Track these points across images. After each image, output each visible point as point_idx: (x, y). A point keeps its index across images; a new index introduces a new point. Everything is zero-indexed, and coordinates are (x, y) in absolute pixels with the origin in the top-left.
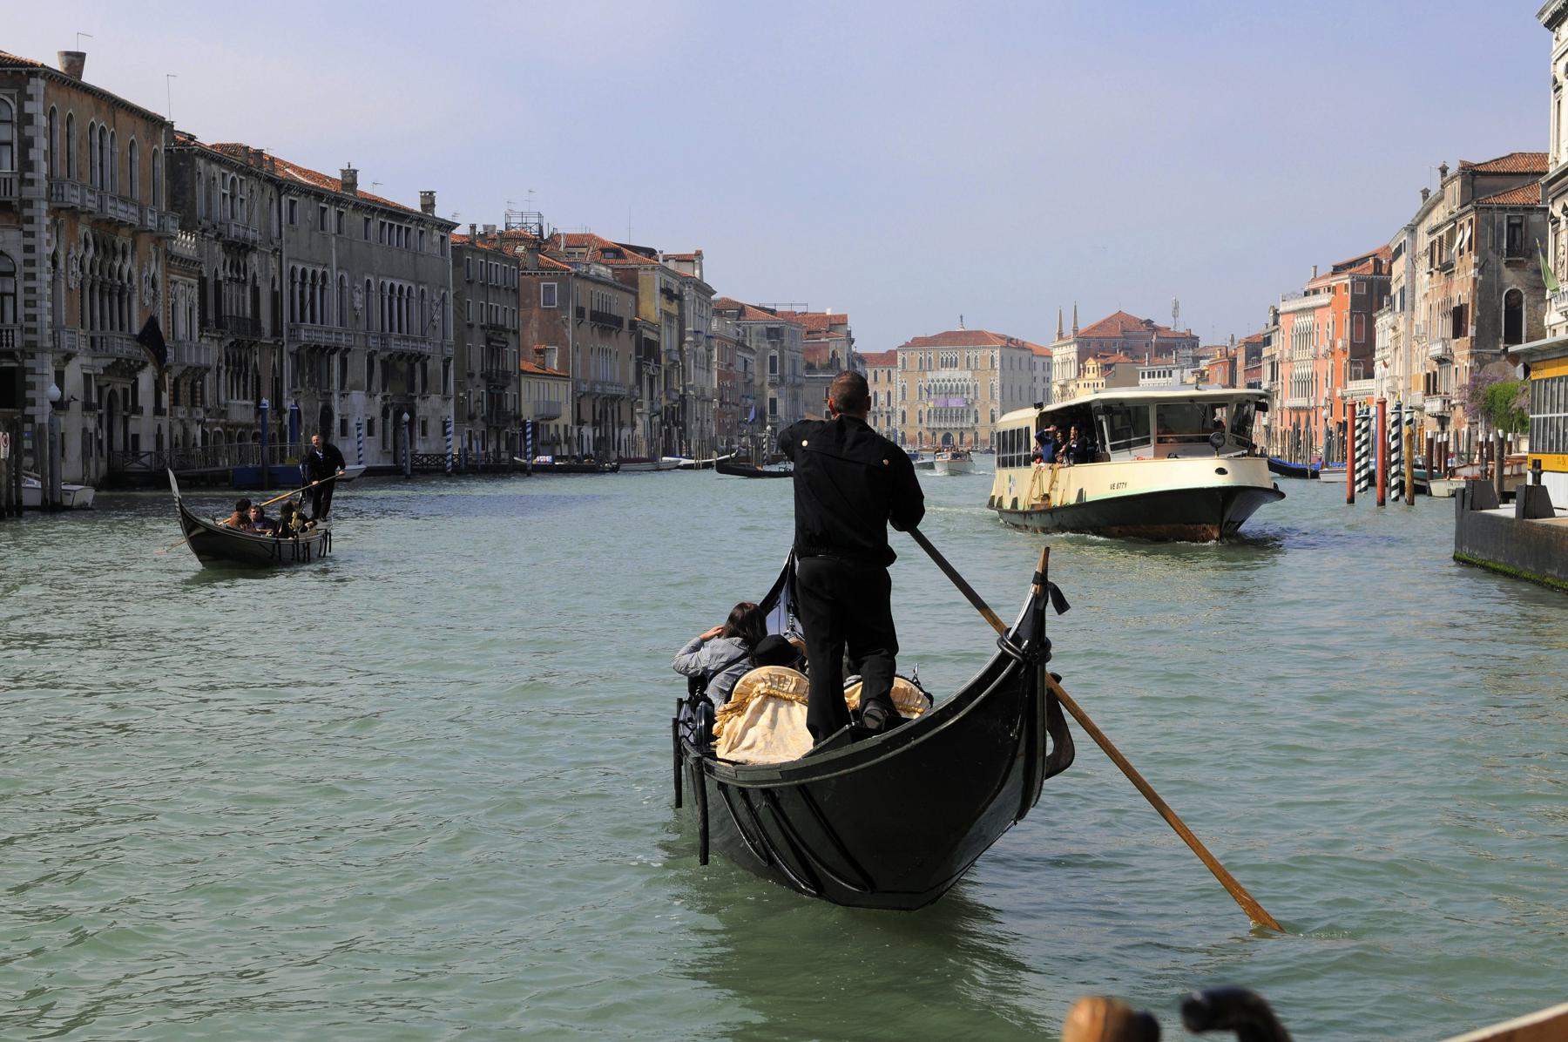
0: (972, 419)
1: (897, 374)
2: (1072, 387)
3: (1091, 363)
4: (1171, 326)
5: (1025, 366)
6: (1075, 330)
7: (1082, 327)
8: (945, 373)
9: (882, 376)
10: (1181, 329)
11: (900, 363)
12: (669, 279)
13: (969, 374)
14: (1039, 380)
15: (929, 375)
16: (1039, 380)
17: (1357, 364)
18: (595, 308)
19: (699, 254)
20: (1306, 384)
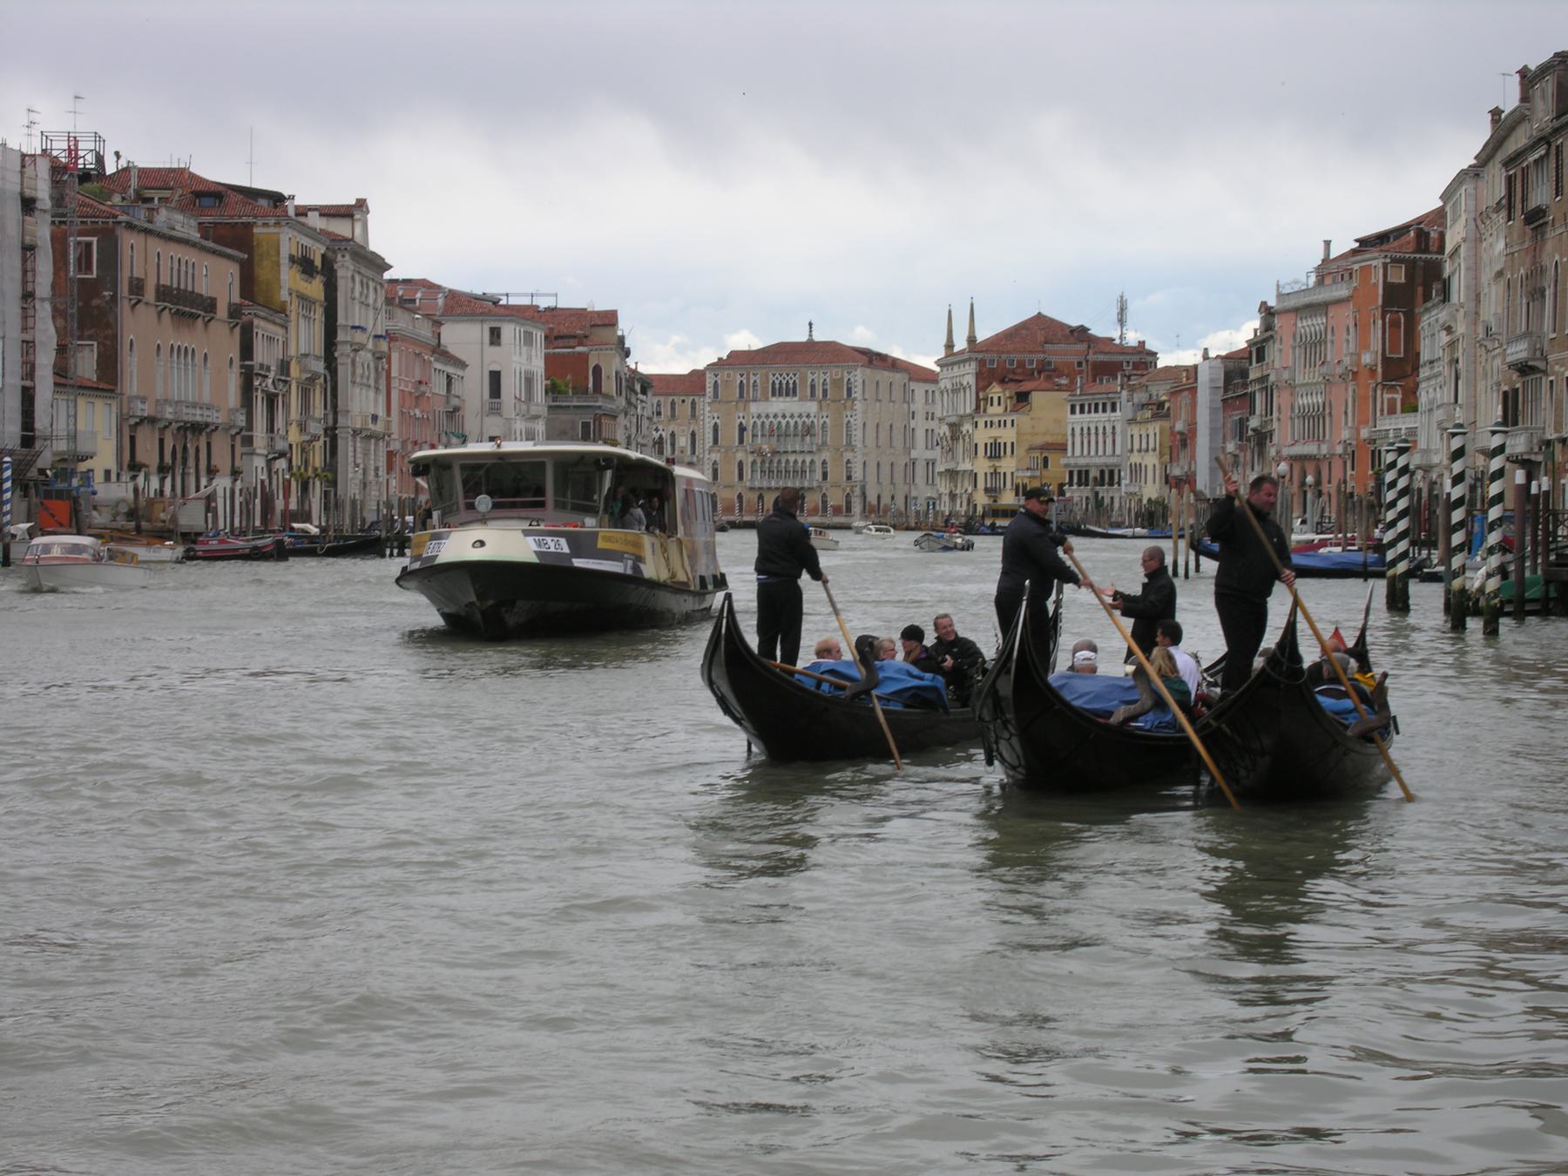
0: (818, 475)
1: (705, 405)
2: (967, 427)
3: (996, 391)
4: (1115, 334)
5: (897, 394)
6: (971, 340)
7: (982, 336)
8: (778, 405)
9: (684, 410)
10: (1132, 339)
11: (709, 390)
12: (306, 241)
13: (812, 407)
14: (920, 416)
15: (754, 408)
16: (920, 416)
17: (1392, 389)
18: (165, 281)
19: (361, 204)
20: (1315, 420)
